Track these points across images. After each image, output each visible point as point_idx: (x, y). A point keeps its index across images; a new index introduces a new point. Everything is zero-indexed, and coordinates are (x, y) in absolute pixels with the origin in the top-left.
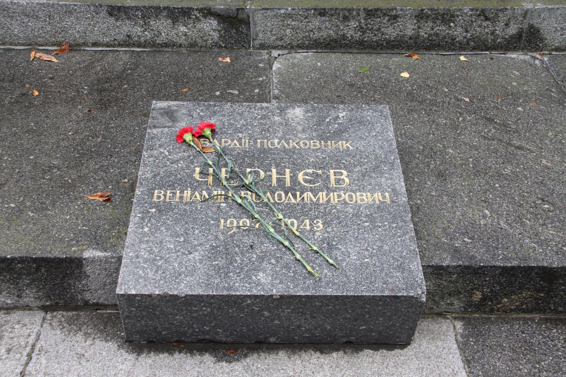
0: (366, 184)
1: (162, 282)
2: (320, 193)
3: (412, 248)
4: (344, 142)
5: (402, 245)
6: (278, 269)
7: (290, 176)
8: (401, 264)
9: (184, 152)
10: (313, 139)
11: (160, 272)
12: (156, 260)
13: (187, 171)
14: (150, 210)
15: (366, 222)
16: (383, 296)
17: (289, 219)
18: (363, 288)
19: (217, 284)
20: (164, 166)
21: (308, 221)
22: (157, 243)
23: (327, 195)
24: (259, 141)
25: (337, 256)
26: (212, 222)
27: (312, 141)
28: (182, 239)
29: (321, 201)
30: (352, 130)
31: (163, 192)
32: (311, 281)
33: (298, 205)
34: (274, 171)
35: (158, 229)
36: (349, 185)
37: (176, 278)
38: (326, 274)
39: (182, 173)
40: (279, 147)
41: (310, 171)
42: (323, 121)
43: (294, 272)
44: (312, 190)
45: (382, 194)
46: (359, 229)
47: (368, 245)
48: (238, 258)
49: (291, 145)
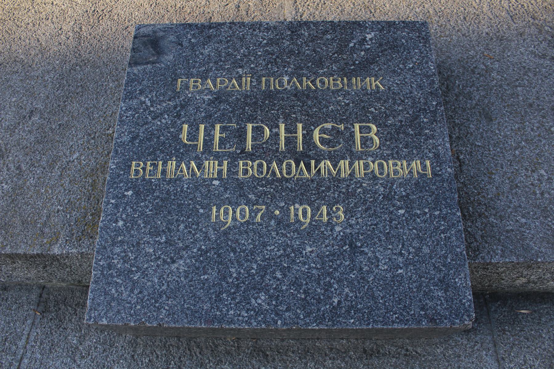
0: (401, 146)
1: (138, 307)
2: (343, 161)
3: (458, 250)
4: (373, 79)
6: (284, 288)
7: (303, 135)
8: (444, 277)
9: (170, 100)
10: (333, 76)
11: (136, 292)
12: (131, 271)
13: (172, 130)
14: (126, 193)
15: (401, 208)
17: (301, 204)
18: (394, 316)
21: (324, 208)
22: (133, 246)
23: (351, 164)
25: (363, 266)
26: (201, 211)
27: (331, 78)
29: (343, 175)
30: (383, 59)
32: (328, 307)
33: (312, 181)
34: (282, 127)
36: (379, 148)
37: (156, 302)
40: (289, 88)
41: (329, 126)
43: (305, 292)
45: (421, 163)
46: (391, 221)
47: (403, 247)
48: (233, 270)
49: (305, 84)
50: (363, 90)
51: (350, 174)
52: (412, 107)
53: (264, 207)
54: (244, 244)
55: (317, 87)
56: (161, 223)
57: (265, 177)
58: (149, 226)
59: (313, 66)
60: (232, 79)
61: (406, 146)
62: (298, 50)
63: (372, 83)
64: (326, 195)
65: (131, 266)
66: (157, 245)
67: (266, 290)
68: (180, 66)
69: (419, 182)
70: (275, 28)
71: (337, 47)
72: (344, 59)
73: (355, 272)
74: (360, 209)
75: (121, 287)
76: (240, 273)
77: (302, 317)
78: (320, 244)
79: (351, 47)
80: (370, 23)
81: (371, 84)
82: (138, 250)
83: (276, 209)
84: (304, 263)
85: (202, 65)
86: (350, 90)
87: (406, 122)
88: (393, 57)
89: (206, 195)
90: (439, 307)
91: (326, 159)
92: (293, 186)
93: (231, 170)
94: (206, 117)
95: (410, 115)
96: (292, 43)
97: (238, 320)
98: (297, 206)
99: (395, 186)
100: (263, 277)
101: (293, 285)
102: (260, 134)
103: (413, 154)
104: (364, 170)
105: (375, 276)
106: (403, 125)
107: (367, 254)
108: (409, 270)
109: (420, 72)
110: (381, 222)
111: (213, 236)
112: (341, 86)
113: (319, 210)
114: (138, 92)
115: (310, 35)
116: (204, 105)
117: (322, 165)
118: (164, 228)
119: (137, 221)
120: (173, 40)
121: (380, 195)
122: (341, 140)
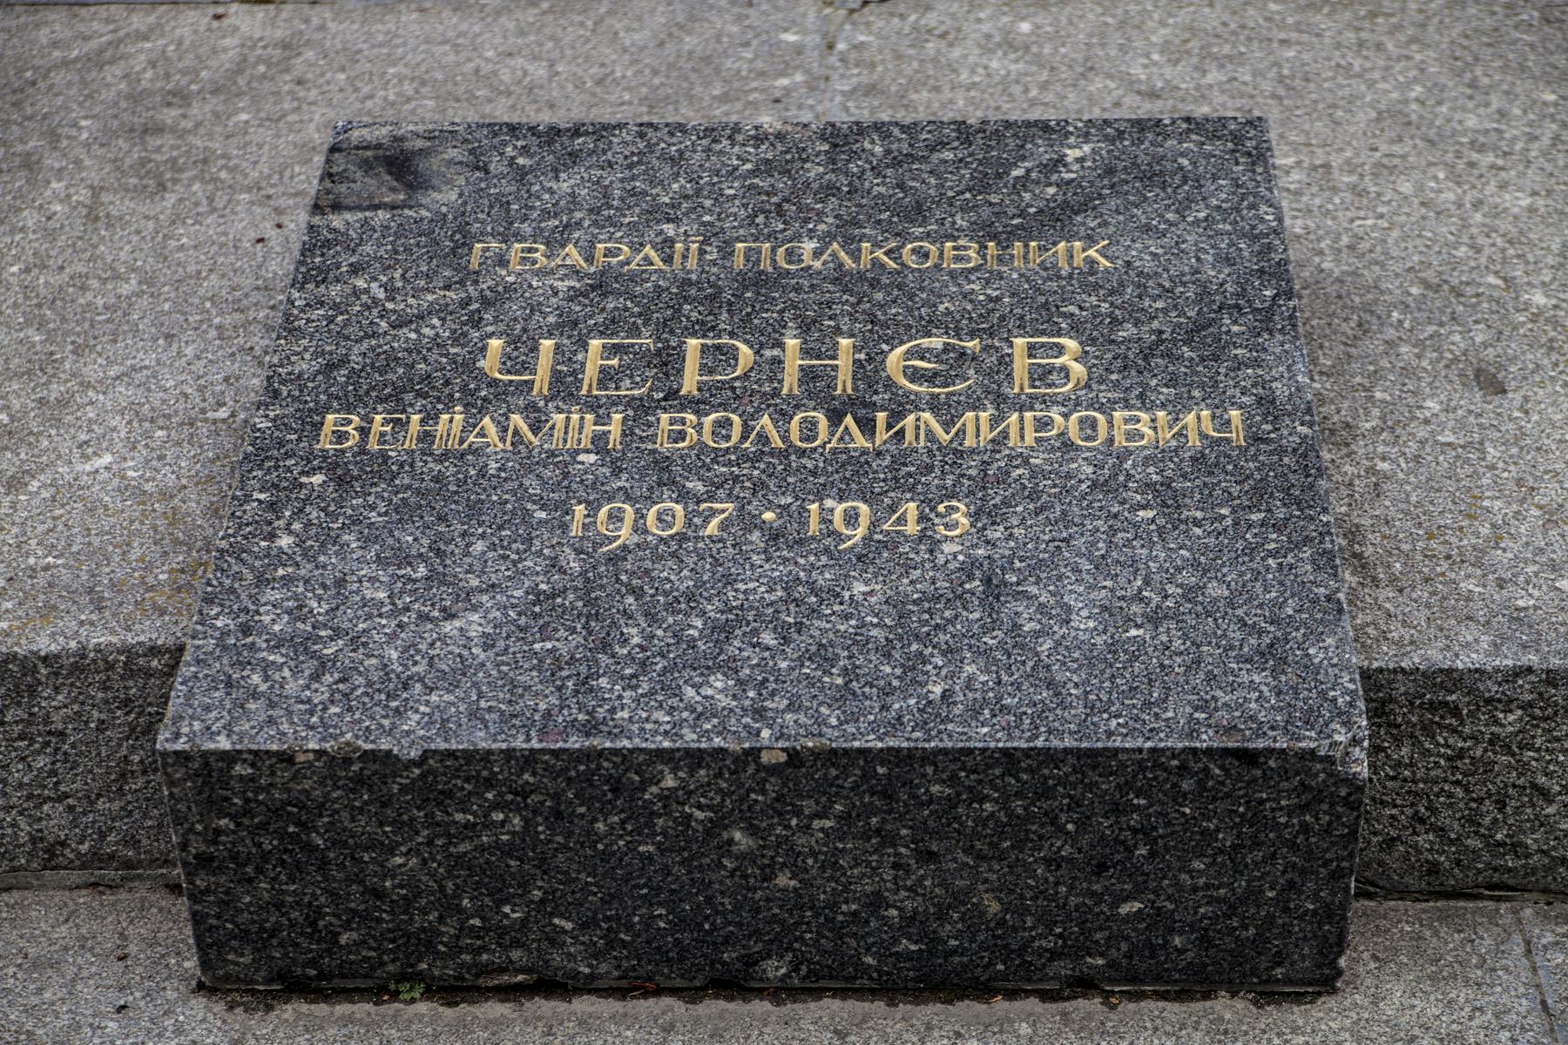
0: (1154, 382)
2: (970, 415)
5: (1281, 583)
6: (784, 665)
8: (1272, 645)
9: (447, 287)
10: (955, 239)
11: (328, 679)
14: (304, 480)
15: (1144, 508)
16: (1194, 751)
17: (841, 500)
18: (1114, 723)
19: (548, 714)
20: (366, 336)
22: (324, 586)
23: (995, 421)
26: (543, 515)
27: (949, 244)
28: (422, 571)
29: (969, 442)
32: (912, 702)
33: (879, 454)
34: (792, 343)
35: (329, 539)
36: (1088, 386)
38: (971, 678)
39: (432, 357)
40: (817, 264)
41: (936, 342)
42: (999, 176)
44: (935, 405)
45: (1213, 417)
46: (1113, 531)
47: (1147, 582)
48: (634, 631)
49: (866, 259)
50: (1046, 269)
53: (730, 506)
57: (736, 448)
59: (895, 219)
61: (1172, 381)
65: (314, 627)
69: (1203, 455)
70: (780, 136)
71: (972, 178)
72: (991, 204)
77: (834, 721)
80: (1080, 125)
83: (768, 509)
84: (847, 617)
85: (546, 214)
90: (1253, 705)
93: (633, 433)
94: (558, 325)
96: (833, 171)
97: (642, 729)
106: (1163, 341)
109: (1228, 227)
115: (888, 152)
120: (460, 158)
121: (1081, 481)
122: (972, 372)
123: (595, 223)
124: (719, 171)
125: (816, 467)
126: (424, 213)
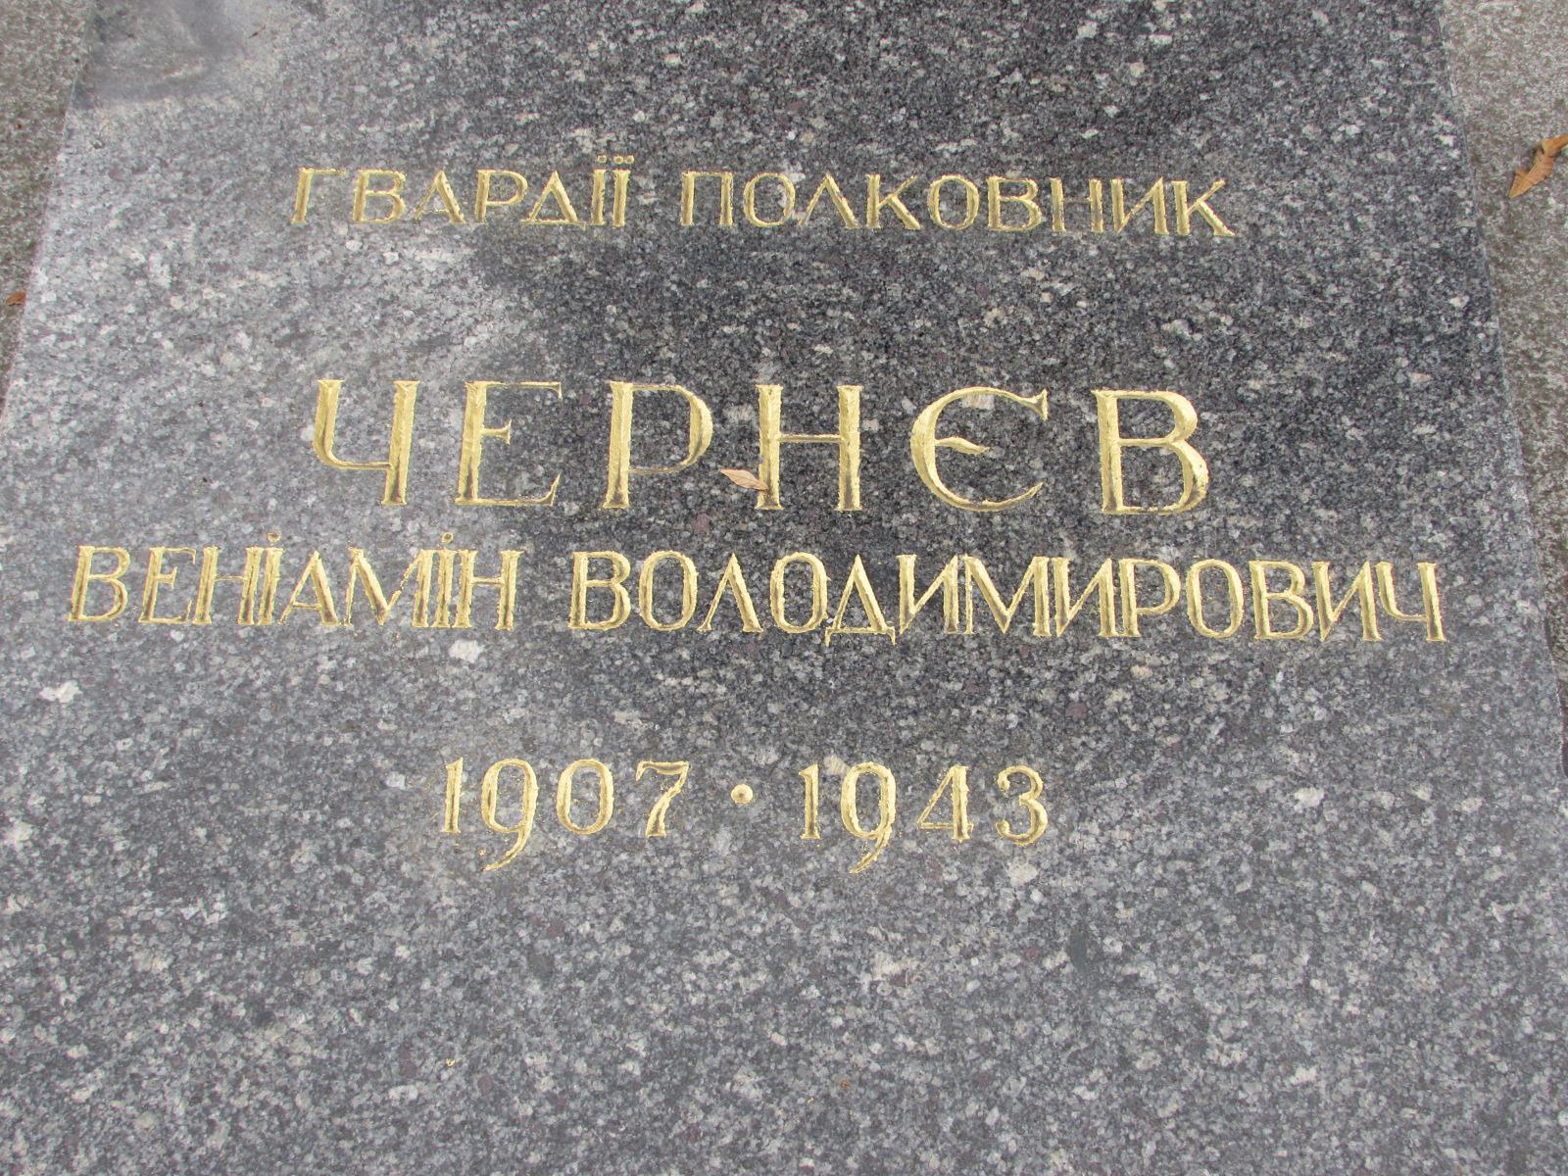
2: (1039, 563)
4: (1182, 186)
6: (773, 1147)
7: (865, 436)
8: (1505, 1104)
9: (257, 267)
12: (61, 1065)
13: (268, 403)
14: (47, 693)
15: (1305, 781)
17: (852, 759)
21: (959, 773)
23: (1080, 576)
24: (690, 177)
25: (1132, 1048)
26: (397, 782)
27: (995, 181)
28: (219, 912)
29: (1042, 628)
30: (1227, 99)
31: (126, 563)
33: (905, 649)
34: (772, 397)
36: (1209, 502)
40: (802, 219)
41: (979, 397)
45: (1395, 572)
48: (541, 1061)
49: (875, 204)
50: (1136, 238)
51: (1074, 623)
52: (1359, 317)
53: (684, 768)
54: (590, 938)
55: (926, 221)
56: (209, 836)
57: (690, 631)
58: (153, 851)
59: (914, 124)
60: (547, 175)
62: (846, 50)
63: (1179, 206)
64: (965, 719)
65: (61, 1037)
66: (187, 941)
67: (691, 1155)
68: (312, 109)
69: (1386, 663)
73: (1096, 1074)
74: (1120, 783)
75: (12, 1137)
76: (569, 1074)
78: (936, 941)
79: (1087, 41)
81: (1172, 214)
82: (96, 960)
83: (741, 776)
84: (867, 1033)
86: (1077, 235)
87: (1327, 386)
88: (1273, 90)
89: (420, 709)
91: (967, 550)
92: (819, 674)
93: (534, 596)
95: (1348, 353)
96: (822, 19)
98: (834, 764)
99: (1280, 677)
100: (674, 1096)
101: (814, 1134)
102: (670, 432)
103: (1362, 531)
104: (1140, 603)
105: (1187, 1095)
106: (1313, 402)
107: (1151, 992)
108: (1343, 1068)
109: (1392, 158)
110: (1216, 844)
111: (446, 901)
112: (1041, 219)
113: (934, 787)
114: (113, 224)
116: (417, 292)
117: (949, 575)
118: (221, 861)
119: (98, 823)
121: (1209, 720)
122: (1038, 464)
123: (477, 128)
124: (655, 16)
125: (812, 679)
126: (234, 104)
